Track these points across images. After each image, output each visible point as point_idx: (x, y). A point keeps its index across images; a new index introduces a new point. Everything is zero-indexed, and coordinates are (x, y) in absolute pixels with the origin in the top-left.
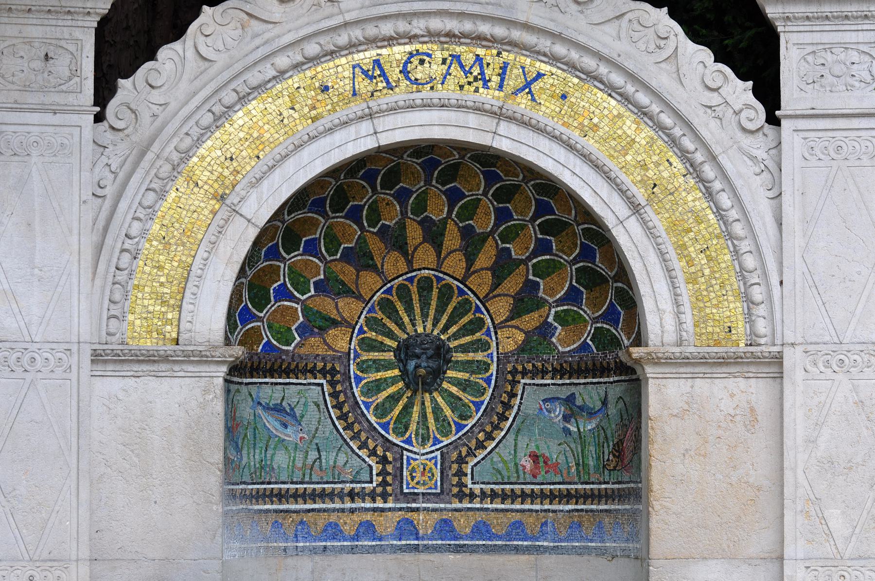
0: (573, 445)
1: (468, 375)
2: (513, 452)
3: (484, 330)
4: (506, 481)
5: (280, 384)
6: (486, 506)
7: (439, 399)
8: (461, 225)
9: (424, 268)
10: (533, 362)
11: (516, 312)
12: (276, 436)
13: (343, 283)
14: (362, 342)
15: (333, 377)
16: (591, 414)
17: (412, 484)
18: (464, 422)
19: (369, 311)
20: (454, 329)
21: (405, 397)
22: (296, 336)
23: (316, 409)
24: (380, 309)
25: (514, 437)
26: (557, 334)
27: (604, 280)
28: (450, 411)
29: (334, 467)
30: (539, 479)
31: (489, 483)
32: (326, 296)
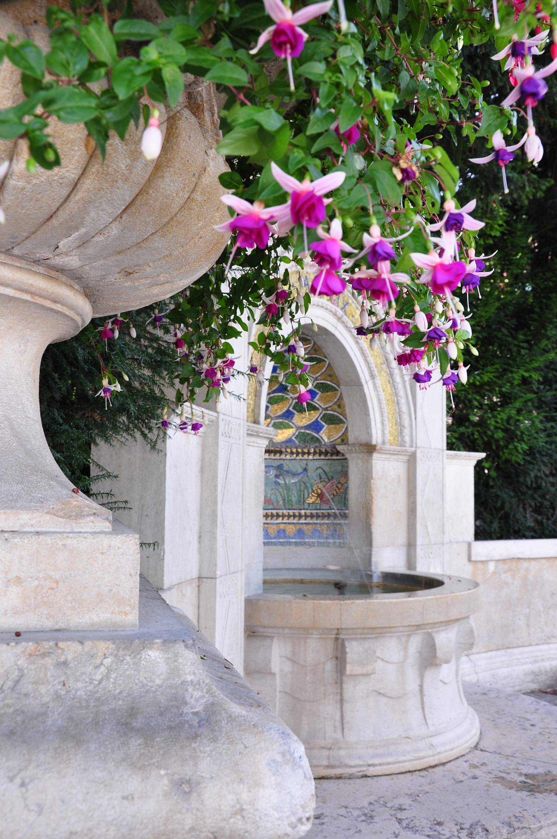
0: (281, 490)
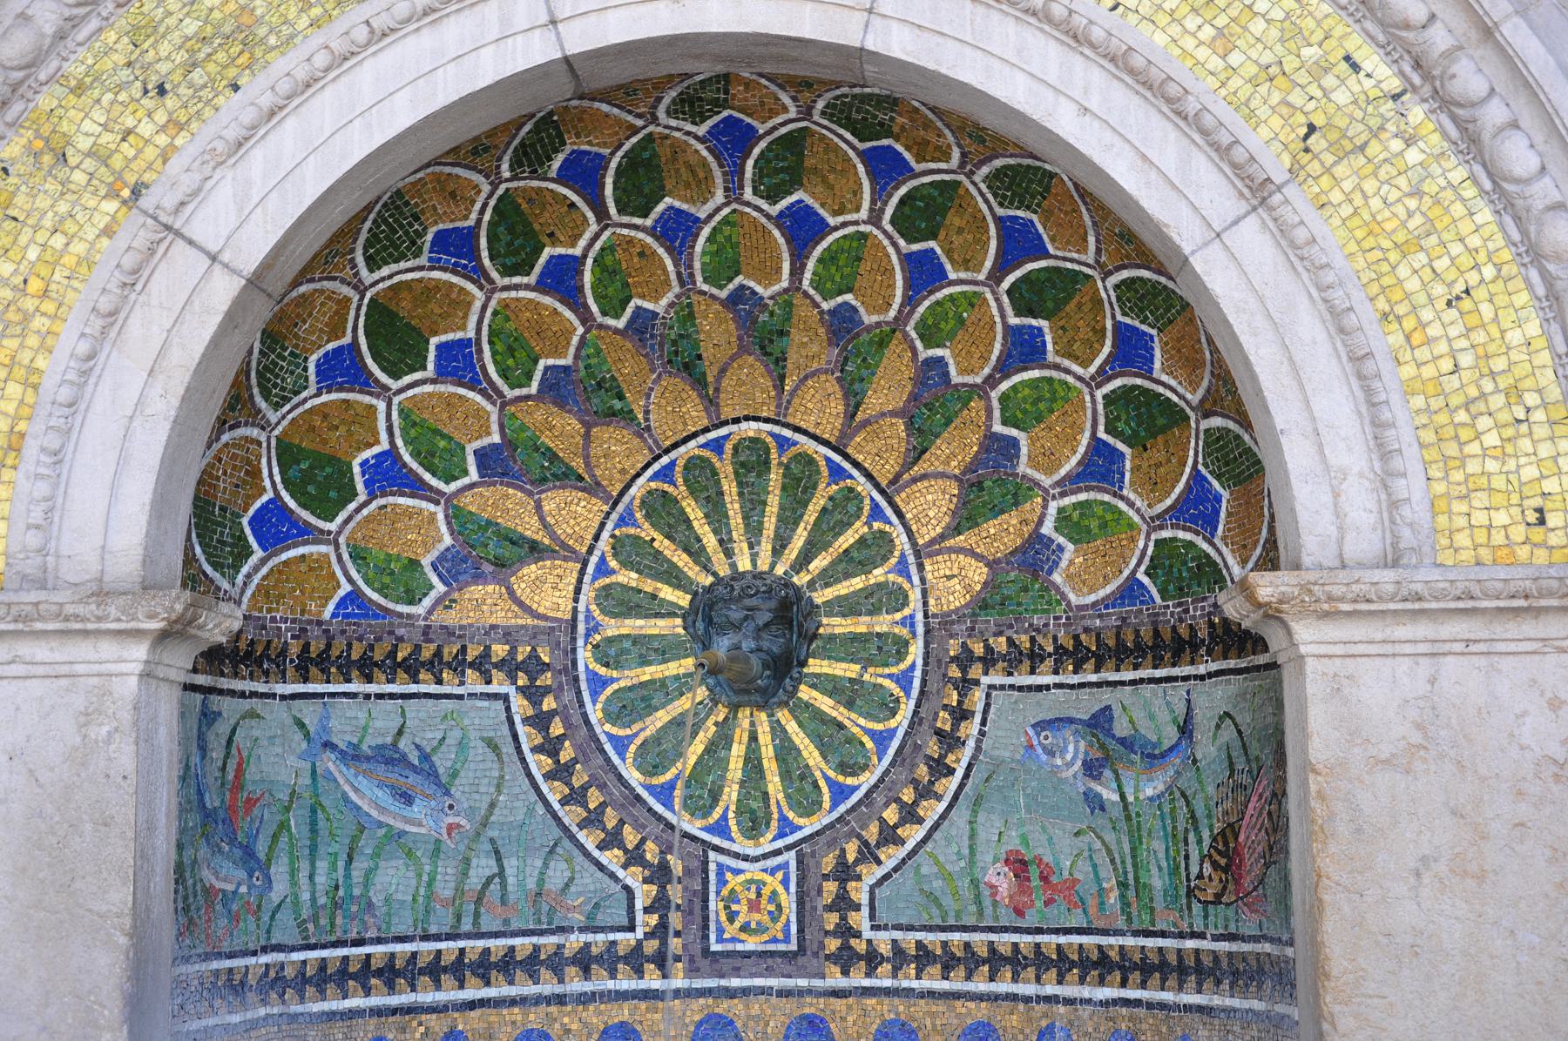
0: (1110, 837)
1: (858, 667)
2: (966, 851)
3: (893, 561)
4: (952, 922)
5: (392, 696)
6: (905, 984)
7: (792, 727)
8: (825, 306)
9: (747, 418)
10: (1010, 633)
11: (965, 517)
12: (380, 825)
13: (553, 456)
14: (605, 593)
15: (532, 679)
16: (1152, 756)
17: (731, 931)
18: (850, 781)
19: (622, 521)
20: (819, 563)
21: (710, 722)
22: (435, 580)
23: (491, 756)
24: (647, 516)
25: (967, 815)
26: (1064, 564)
27: (1177, 417)
28: (816, 753)
29: (539, 894)
30: (1031, 920)
31: (911, 928)
32: (509, 485)
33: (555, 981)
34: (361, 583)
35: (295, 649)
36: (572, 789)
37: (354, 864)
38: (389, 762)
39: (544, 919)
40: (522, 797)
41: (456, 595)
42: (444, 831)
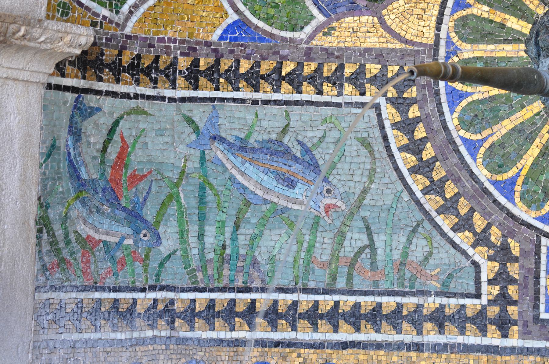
5: (277, 102)
12: (265, 202)
14: (463, 22)
22: (315, 11)
23: (364, 152)
29: (403, 264)
33: (415, 332)
34: (248, 14)
35: (183, 63)
36: (432, 182)
37: (240, 231)
38: (274, 153)
39: (406, 283)
40: (390, 186)
41: (335, 24)
42: (322, 210)
